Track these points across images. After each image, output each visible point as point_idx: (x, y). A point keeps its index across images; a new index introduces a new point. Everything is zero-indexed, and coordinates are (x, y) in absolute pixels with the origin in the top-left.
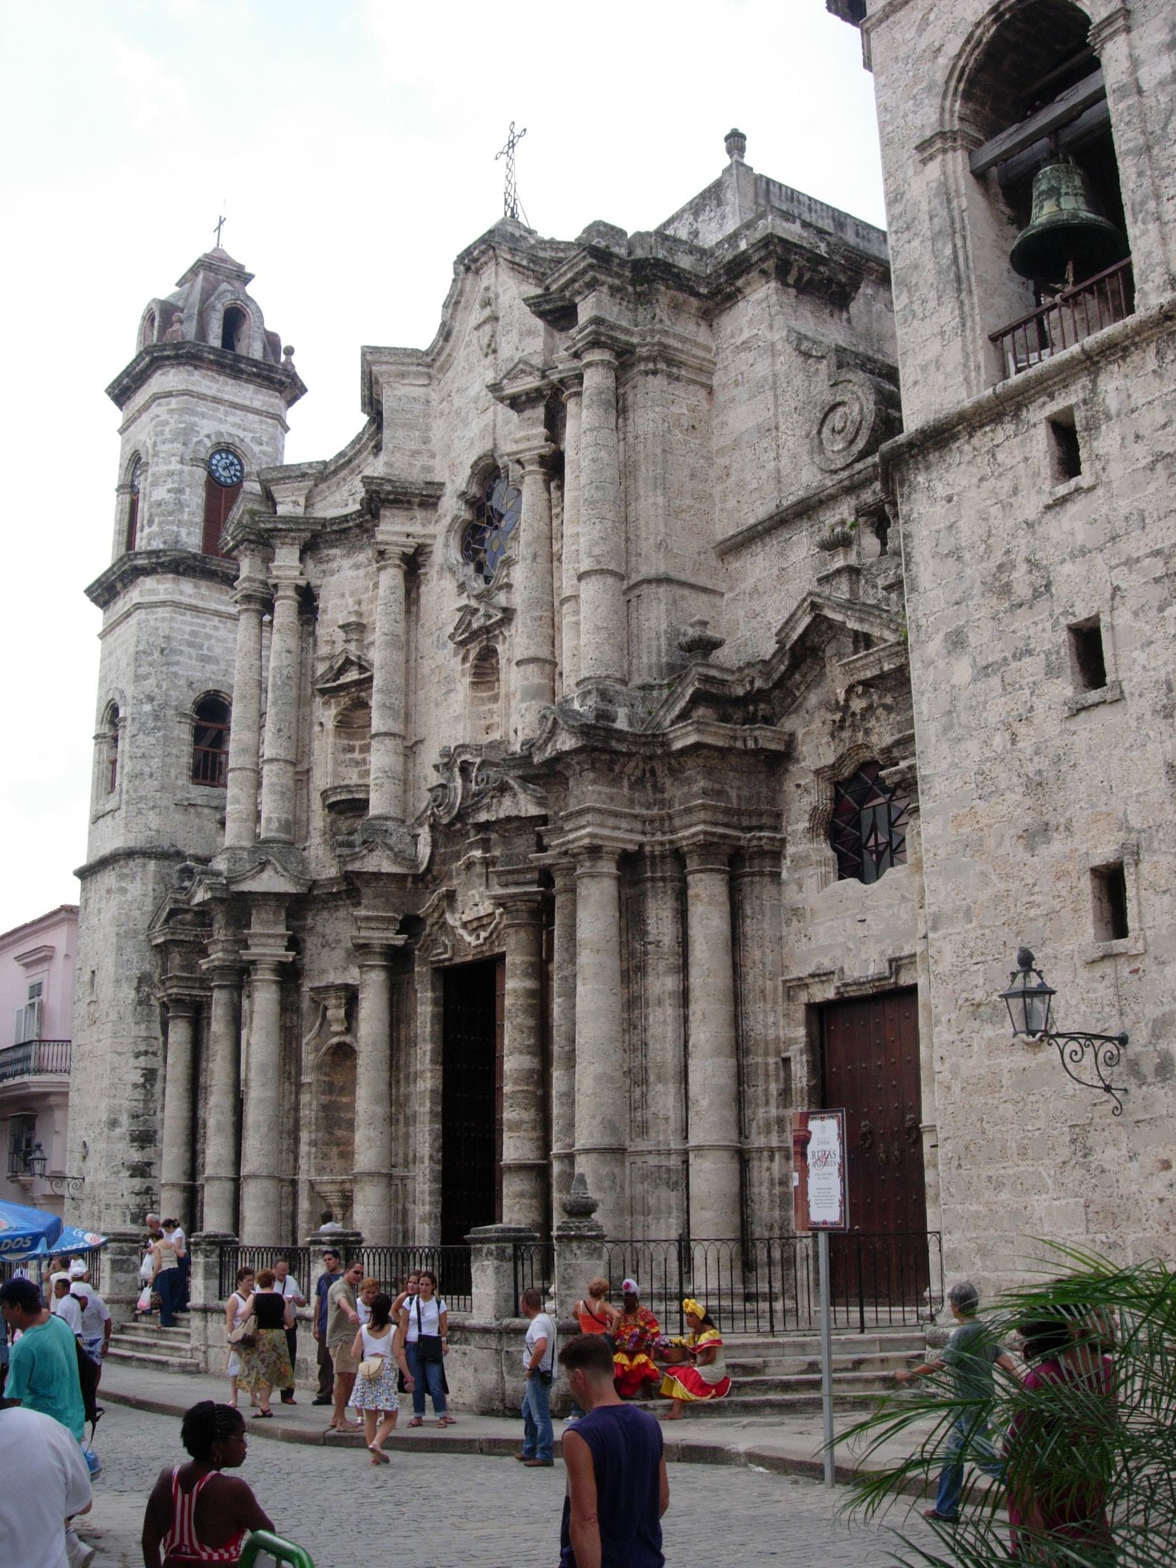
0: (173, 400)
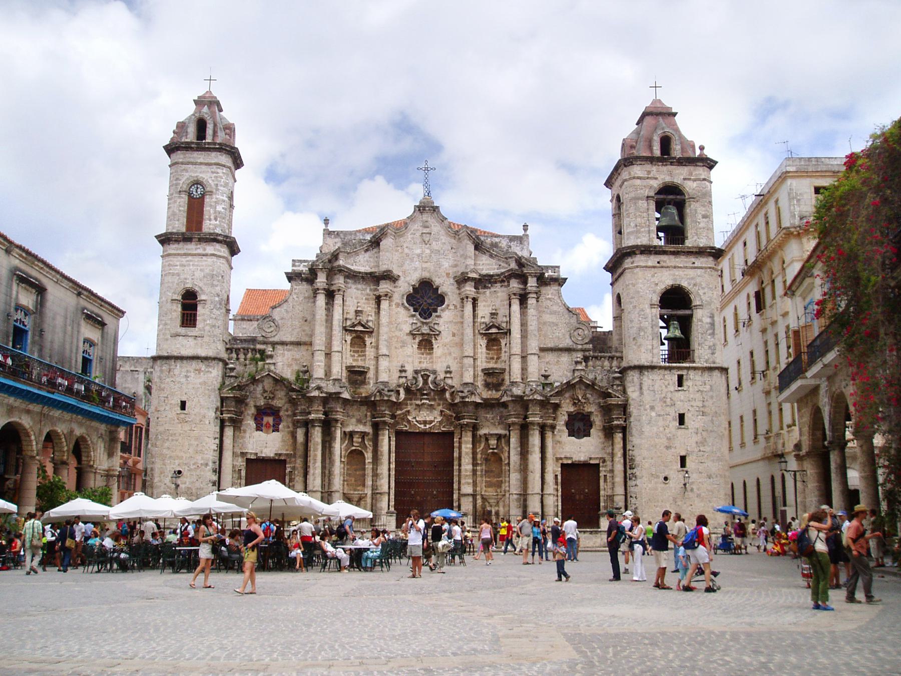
0: (225, 169)
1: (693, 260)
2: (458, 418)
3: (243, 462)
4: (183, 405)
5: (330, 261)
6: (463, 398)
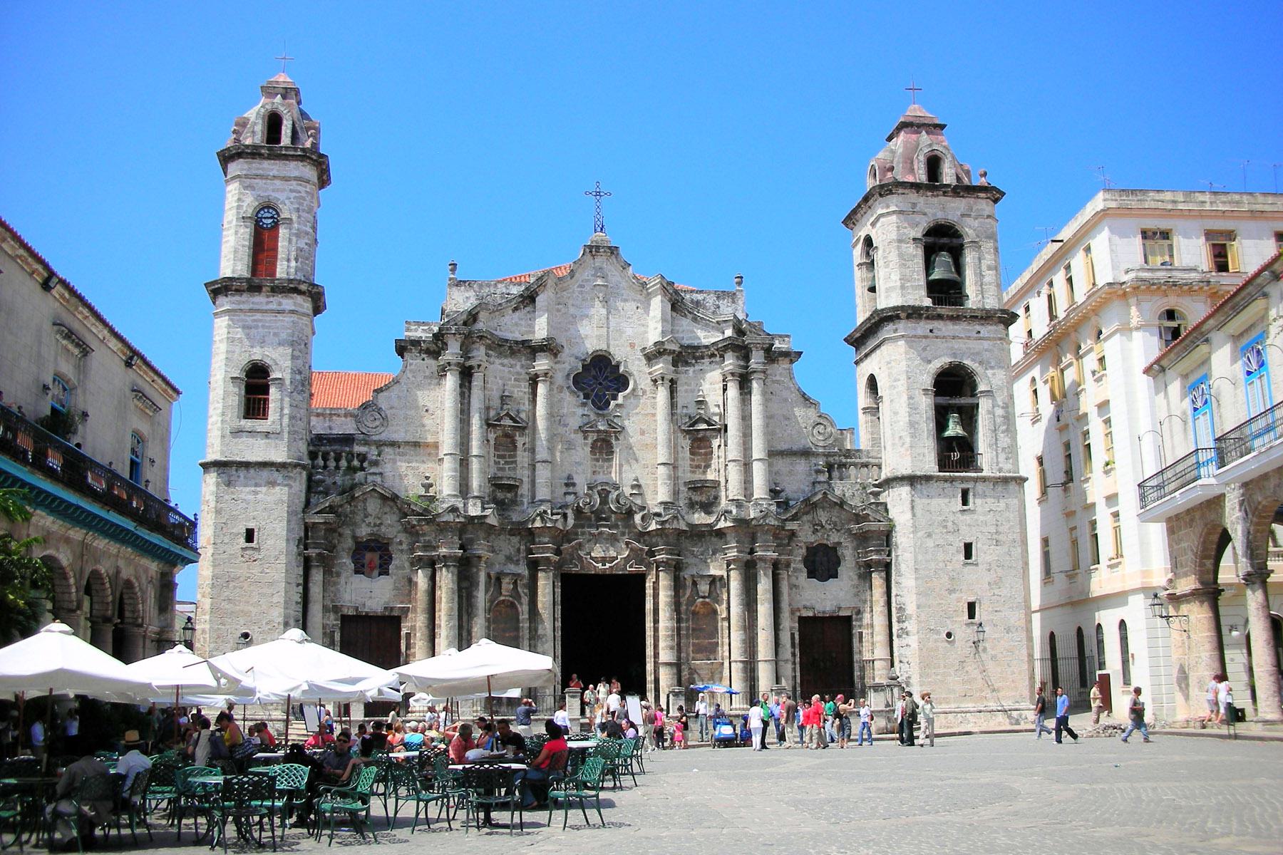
1: (978, 328)
2: (651, 554)
3: (336, 620)
4: (250, 535)
5: (465, 324)
6: (663, 523)
